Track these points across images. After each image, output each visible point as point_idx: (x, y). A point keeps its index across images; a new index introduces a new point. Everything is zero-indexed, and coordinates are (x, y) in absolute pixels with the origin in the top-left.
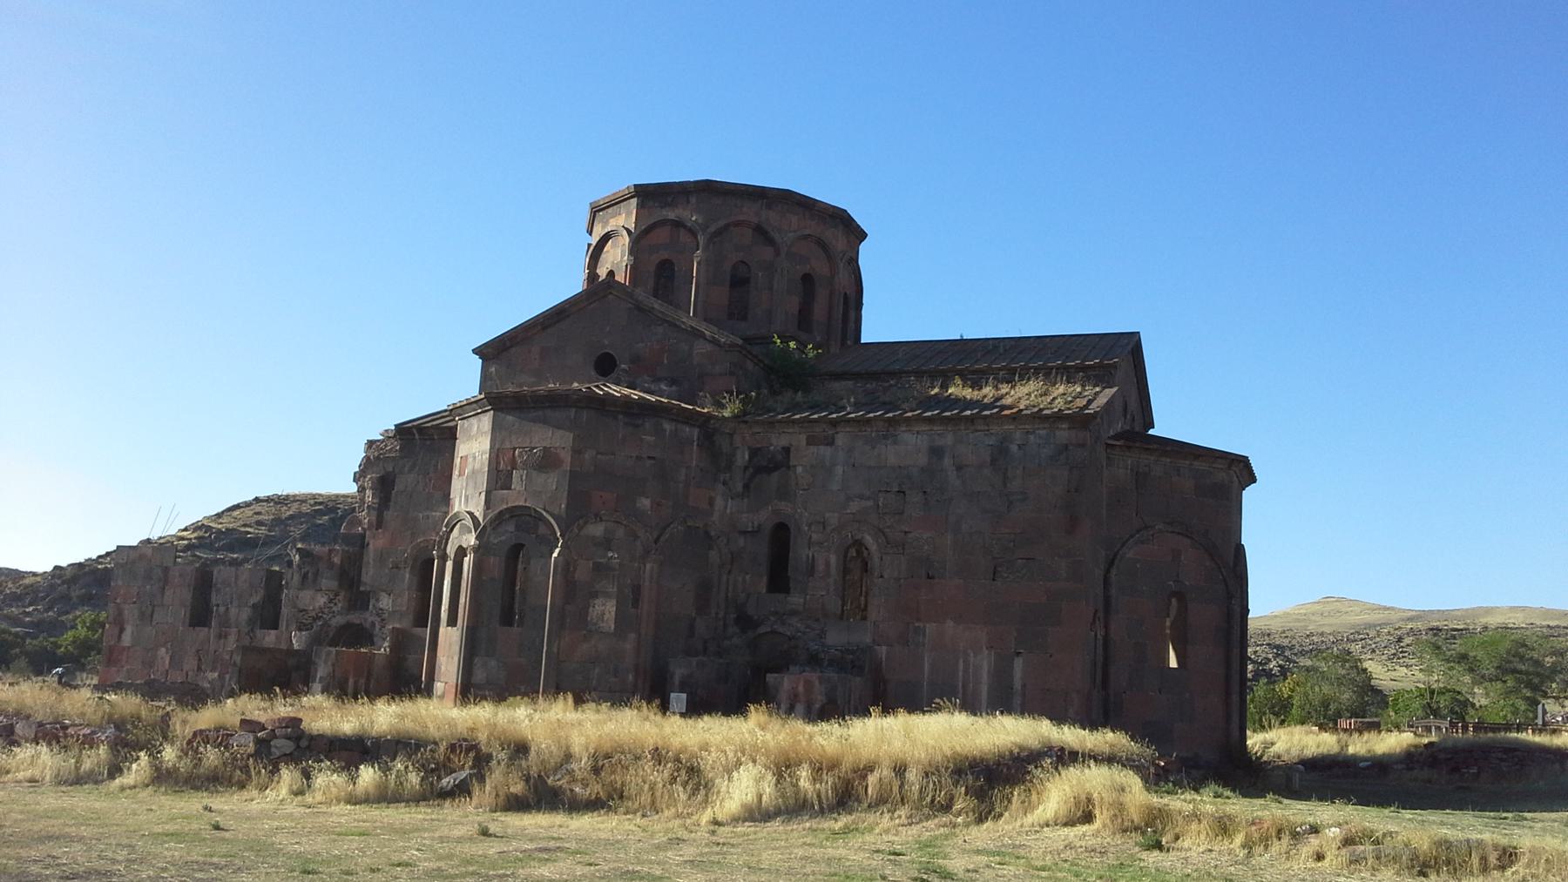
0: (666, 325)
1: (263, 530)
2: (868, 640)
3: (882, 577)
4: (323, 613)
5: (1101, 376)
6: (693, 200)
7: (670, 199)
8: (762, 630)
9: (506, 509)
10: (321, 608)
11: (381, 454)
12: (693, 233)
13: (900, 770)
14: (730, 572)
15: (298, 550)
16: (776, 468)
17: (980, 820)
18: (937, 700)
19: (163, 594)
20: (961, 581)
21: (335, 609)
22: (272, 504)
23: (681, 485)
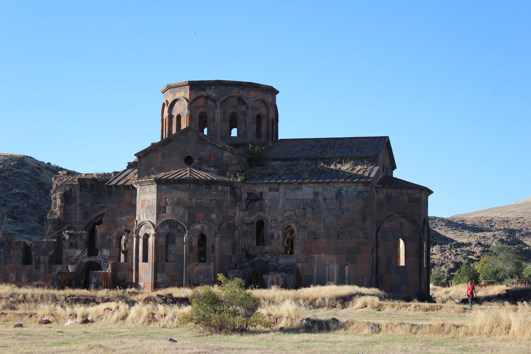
0: (212, 145)
2: (294, 261)
3: (298, 239)
4: (79, 257)
5: (373, 160)
6: (213, 88)
7: (203, 87)
8: (256, 259)
10: (78, 256)
12: (214, 101)
14: (242, 238)
15: (67, 233)
16: (258, 200)
17: (343, 309)
18: (329, 282)
20: (326, 240)
21: (84, 256)
23: (225, 208)
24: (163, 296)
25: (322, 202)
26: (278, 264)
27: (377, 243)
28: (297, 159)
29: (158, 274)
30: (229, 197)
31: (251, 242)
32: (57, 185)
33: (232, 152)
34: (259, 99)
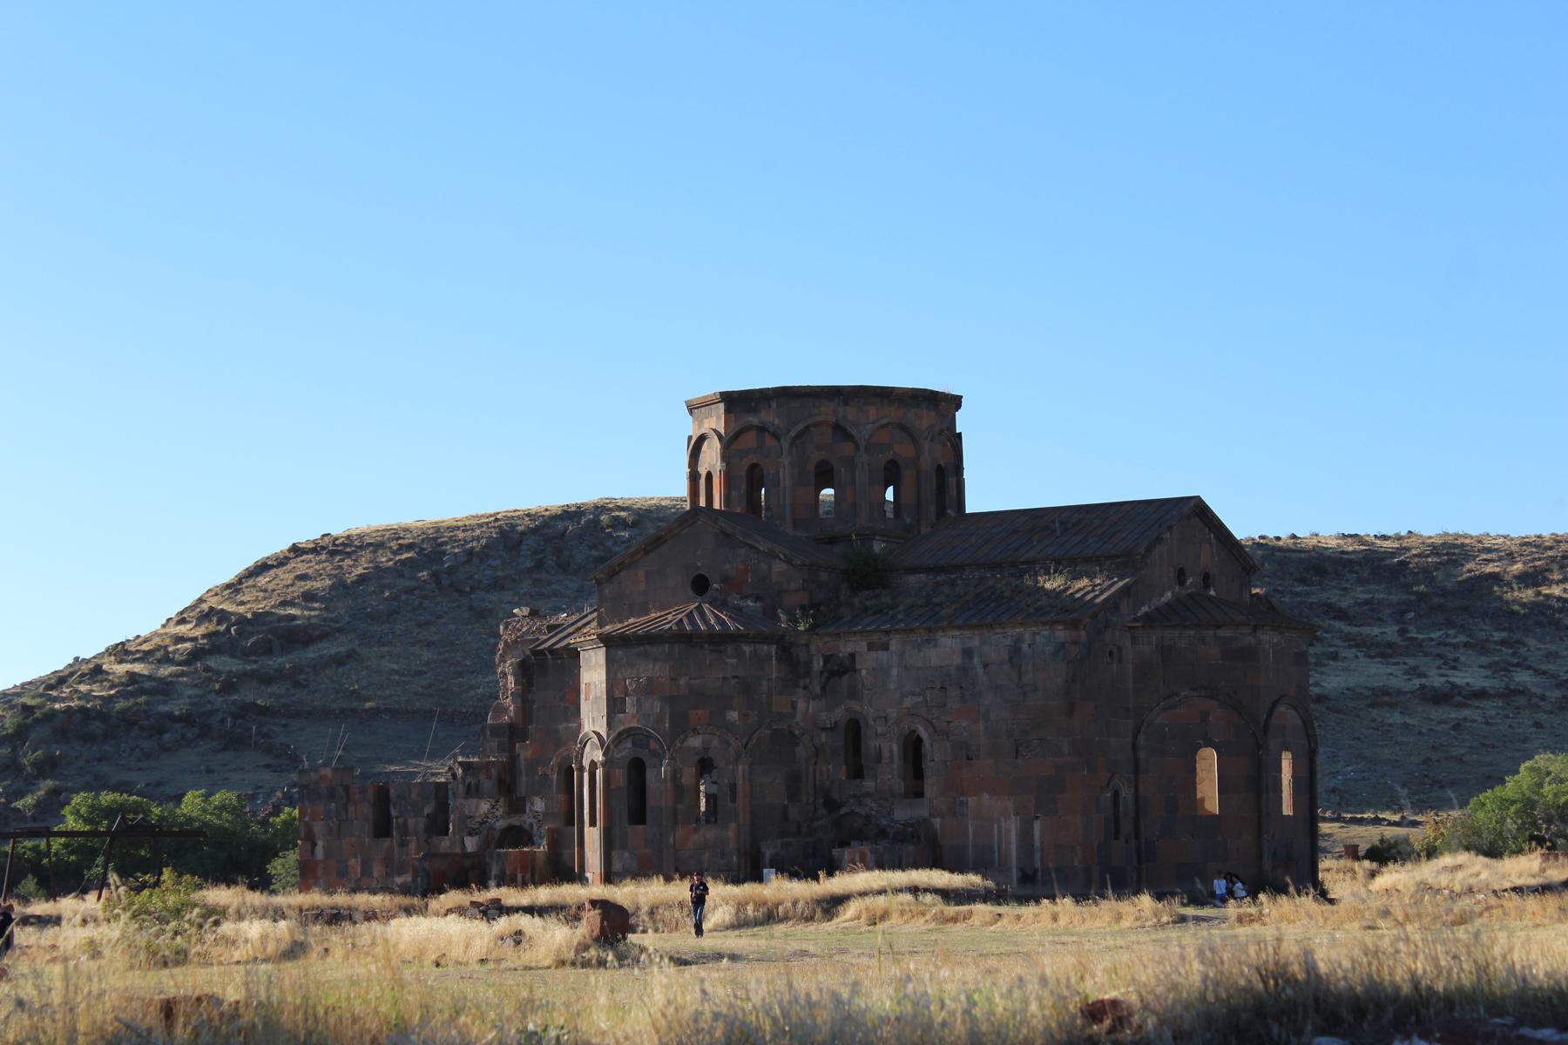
1: (314, 612)
2: (925, 813)
6: (774, 405)
7: (753, 404)
8: (843, 811)
9: (624, 730)
11: (518, 637)
12: (776, 436)
13: (795, 903)
14: (816, 763)
15: (461, 764)
16: (845, 672)
19: (347, 812)
21: (497, 813)
22: (323, 557)
23: (764, 696)
24: (482, 905)
25: (980, 671)
26: (892, 821)
27: (1136, 761)
28: (960, 568)
29: (613, 853)
30: (774, 670)
31: (833, 771)
32: (506, 642)
33: (788, 561)
34: (889, 423)
